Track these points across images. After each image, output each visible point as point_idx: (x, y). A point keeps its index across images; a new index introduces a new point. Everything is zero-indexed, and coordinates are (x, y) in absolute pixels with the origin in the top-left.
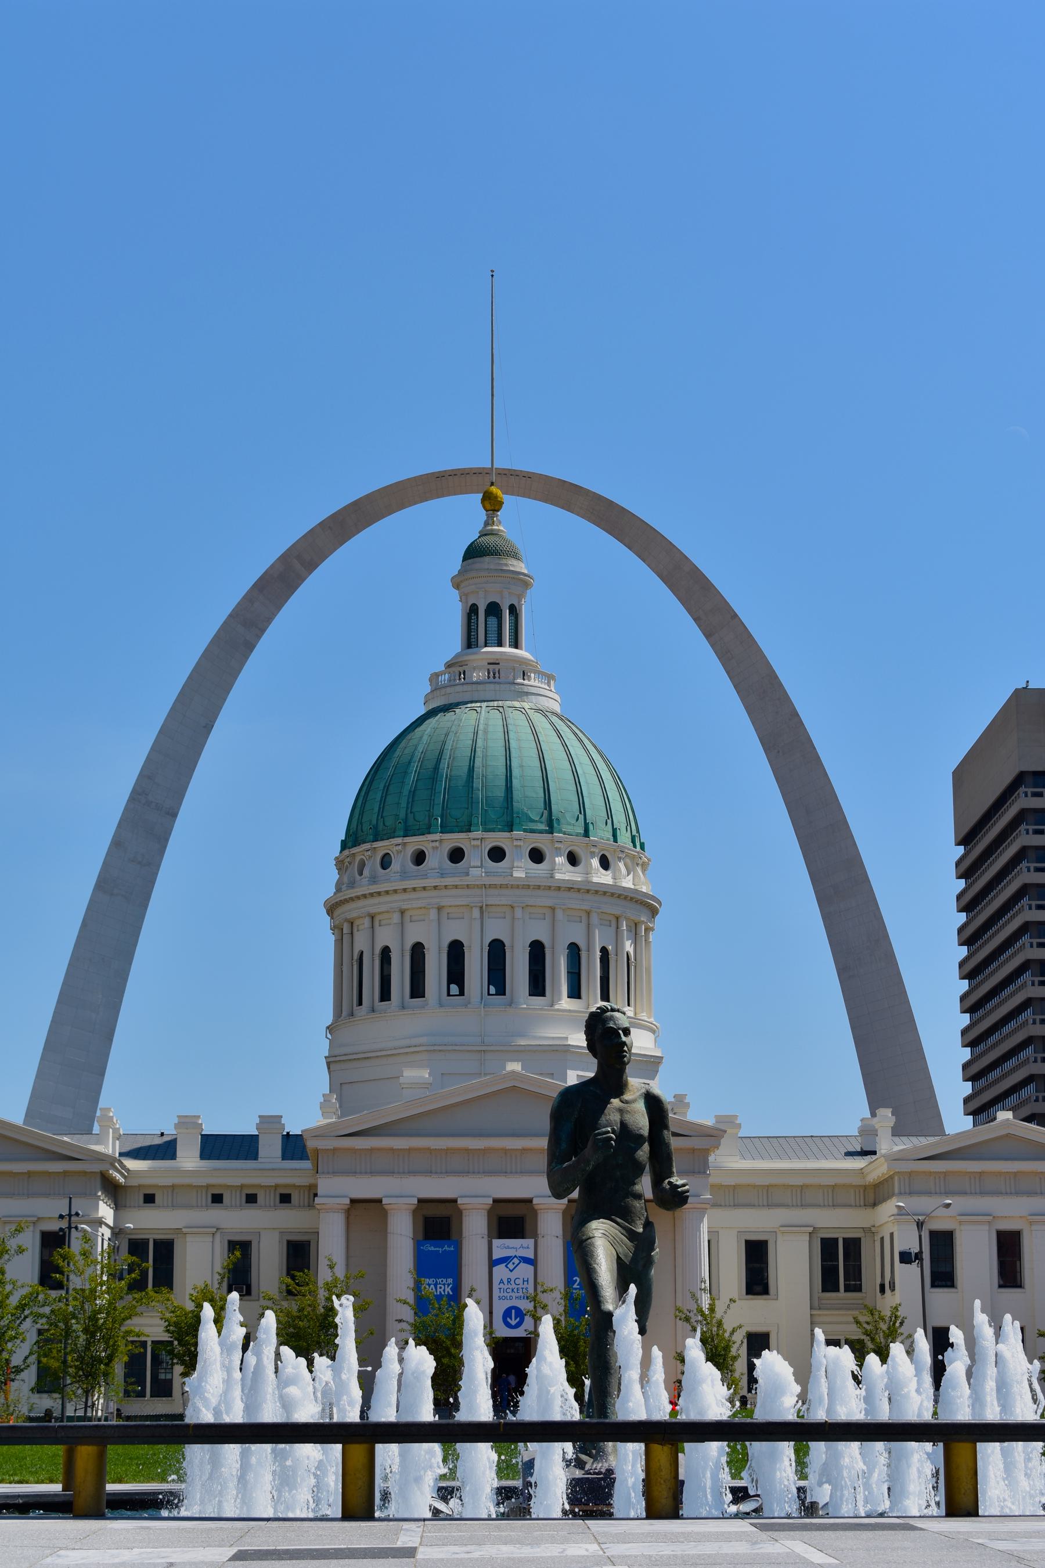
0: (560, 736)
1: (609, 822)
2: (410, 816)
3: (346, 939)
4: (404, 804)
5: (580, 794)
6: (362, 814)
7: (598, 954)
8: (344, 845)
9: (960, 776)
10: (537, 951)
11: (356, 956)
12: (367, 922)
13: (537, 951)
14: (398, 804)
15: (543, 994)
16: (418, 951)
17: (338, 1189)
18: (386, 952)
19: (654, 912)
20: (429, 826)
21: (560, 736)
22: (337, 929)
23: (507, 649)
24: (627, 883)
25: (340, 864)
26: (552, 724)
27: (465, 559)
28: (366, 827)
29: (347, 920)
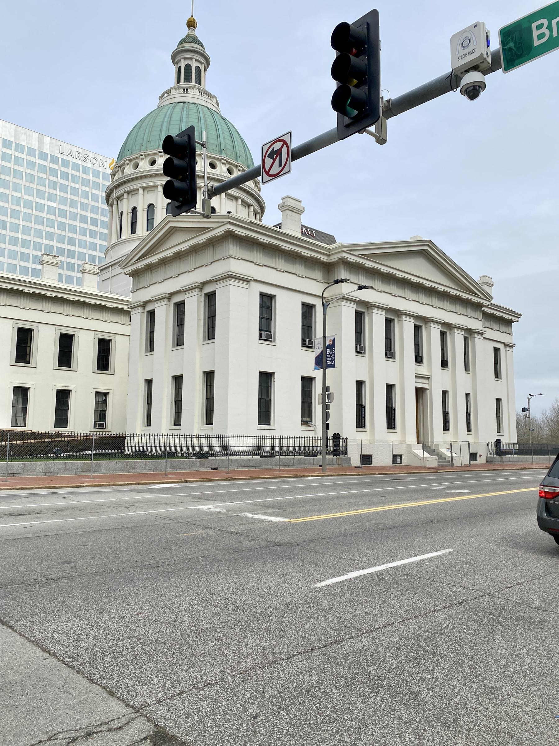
12: (115, 203)
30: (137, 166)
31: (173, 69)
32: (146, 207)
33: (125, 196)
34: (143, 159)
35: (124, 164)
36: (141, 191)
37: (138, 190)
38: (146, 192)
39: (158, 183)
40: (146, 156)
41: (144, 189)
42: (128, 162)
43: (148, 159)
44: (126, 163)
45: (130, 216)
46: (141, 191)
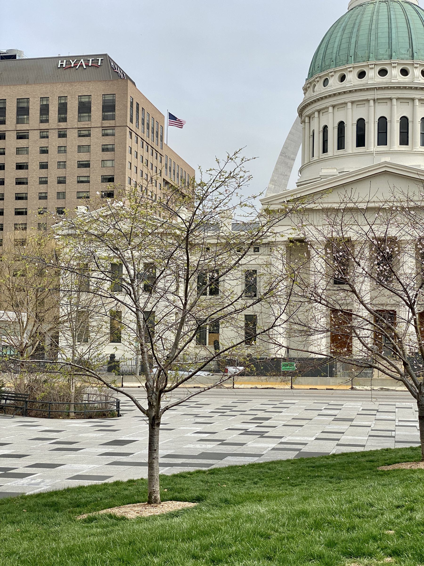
2: (338, 57)
4: (335, 51)
8: (307, 79)
10: (404, 122)
11: (311, 134)
12: (316, 114)
13: (404, 122)
15: (407, 144)
16: (341, 126)
18: (325, 127)
20: (348, 60)
22: (303, 122)
25: (305, 89)
26: (414, 8)
28: (316, 67)
29: (307, 116)
30: (343, 78)
32: (356, 122)
37: (347, 103)
39: (369, 97)
40: (354, 68)
41: (353, 102)
42: (333, 73)
44: (330, 74)
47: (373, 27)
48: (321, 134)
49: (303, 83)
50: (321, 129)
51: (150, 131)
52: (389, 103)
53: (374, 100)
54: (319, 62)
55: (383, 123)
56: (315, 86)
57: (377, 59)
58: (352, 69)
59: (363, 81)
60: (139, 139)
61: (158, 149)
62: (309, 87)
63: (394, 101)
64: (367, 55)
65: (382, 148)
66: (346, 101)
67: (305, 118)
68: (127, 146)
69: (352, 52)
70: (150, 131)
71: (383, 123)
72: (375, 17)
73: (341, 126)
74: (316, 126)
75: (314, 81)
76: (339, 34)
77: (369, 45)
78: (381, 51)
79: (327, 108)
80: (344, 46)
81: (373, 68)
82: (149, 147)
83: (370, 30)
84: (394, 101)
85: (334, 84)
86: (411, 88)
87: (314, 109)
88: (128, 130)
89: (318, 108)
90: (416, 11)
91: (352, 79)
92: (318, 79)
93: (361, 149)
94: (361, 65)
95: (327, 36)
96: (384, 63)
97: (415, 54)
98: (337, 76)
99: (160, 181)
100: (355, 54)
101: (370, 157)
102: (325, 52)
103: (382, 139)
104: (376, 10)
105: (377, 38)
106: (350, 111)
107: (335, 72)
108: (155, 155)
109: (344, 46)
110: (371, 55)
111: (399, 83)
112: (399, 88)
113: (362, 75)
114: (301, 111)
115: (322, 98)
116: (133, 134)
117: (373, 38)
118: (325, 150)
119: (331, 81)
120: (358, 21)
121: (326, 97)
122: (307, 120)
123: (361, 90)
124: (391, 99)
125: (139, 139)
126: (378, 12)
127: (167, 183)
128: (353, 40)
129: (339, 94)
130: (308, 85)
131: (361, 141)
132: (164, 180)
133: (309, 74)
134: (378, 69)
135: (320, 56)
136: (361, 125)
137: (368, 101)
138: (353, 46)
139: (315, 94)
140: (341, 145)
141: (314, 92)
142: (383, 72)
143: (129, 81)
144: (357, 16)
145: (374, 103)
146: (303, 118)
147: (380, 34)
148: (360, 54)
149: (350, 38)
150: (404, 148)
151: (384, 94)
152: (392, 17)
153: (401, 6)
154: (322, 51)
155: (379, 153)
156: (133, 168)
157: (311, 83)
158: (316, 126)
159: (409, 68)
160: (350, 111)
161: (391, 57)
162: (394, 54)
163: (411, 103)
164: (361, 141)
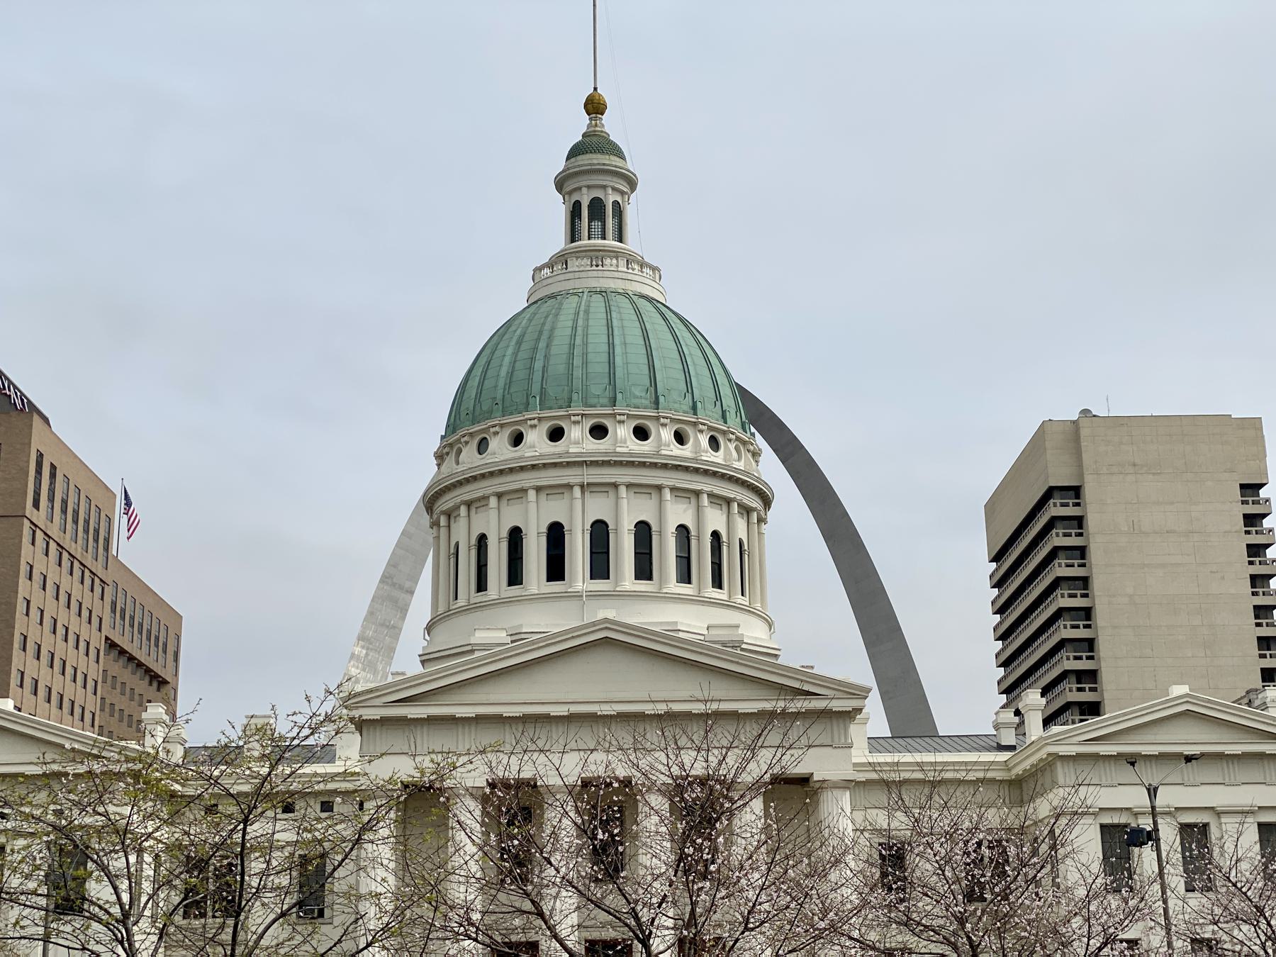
0: (665, 319)
1: (718, 403)
3: (443, 531)
4: (501, 383)
5: (686, 372)
6: (460, 405)
7: (708, 540)
8: (443, 437)
9: (992, 508)
12: (463, 510)
13: (643, 532)
14: (496, 386)
15: (650, 578)
16: (515, 537)
17: (401, 767)
18: (482, 539)
19: (767, 502)
21: (665, 319)
22: (435, 524)
23: (611, 243)
24: (740, 465)
25: (440, 457)
27: (568, 159)
29: (443, 513)
30: (517, 439)
31: (558, 210)
32: (544, 529)
33: (493, 501)
34: (534, 426)
35: (486, 430)
36: (532, 494)
38: (543, 496)
39: (572, 480)
40: (540, 419)
41: (538, 489)
42: (497, 429)
43: (545, 427)
44: (492, 430)
45: (505, 545)
46: (532, 494)
47: (578, 341)
48: (474, 553)
49: (436, 444)
50: (474, 541)
51: (81, 528)
52: (612, 494)
53: (582, 486)
54: (469, 403)
55: (600, 533)
56: (459, 451)
57: (587, 405)
58: (535, 422)
59: (560, 447)
60: (53, 546)
61: (98, 568)
62: (447, 454)
63: (623, 490)
64: (566, 395)
65: (600, 585)
66: (526, 484)
67: (438, 519)
68: (23, 562)
69: (536, 388)
70: (81, 528)
71: (600, 533)
72: (580, 322)
73: (515, 537)
74: (463, 534)
75: (458, 441)
76: (510, 351)
77: (570, 376)
78: (595, 390)
79: (485, 498)
80: (520, 374)
81: (578, 422)
82: (76, 564)
83: (572, 346)
84: (623, 490)
85: (500, 450)
86: (654, 466)
87: (458, 500)
88: (26, 522)
89: (467, 497)
90: (662, 315)
91: (536, 442)
92: (466, 438)
93: (556, 586)
94: (555, 415)
95: (487, 351)
96: (600, 412)
97: (661, 399)
98: (506, 433)
99: (97, 642)
100: (543, 392)
101: (573, 605)
102: (481, 383)
103: (600, 567)
104: (582, 308)
105: (585, 363)
106: (533, 506)
107: (502, 426)
108: (88, 581)
109: (520, 374)
110: (575, 396)
111: (630, 454)
112: (631, 464)
113: (556, 434)
114: (431, 501)
115: (475, 478)
116: (39, 534)
117: (577, 361)
118: (481, 586)
119: (494, 444)
120: (547, 327)
121: (483, 476)
122: (443, 521)
123: (555, 465)
124: (615, 486)
125: (53, 546)
126: (587, 312)
127: (112, 645)
128: (538, 365)
129: (511, 470)
130: (446, 450)
131: (556, 570)
132: (107, 638)
133: (448, 426)
134: (589, 423)
135: (472, 392)
136: (556, 535)
137: (569, 487)
138: (537, 376)
139: (460, 468)
140: (515, 577)
141: (458, 463)
142: (599, 431)
143: (36, 417)
144: (546, 317)
145: (583, 493)
146: (435, 517)
147: (590, 356)
148: (551, 392)
149: (532, 359)
150: (643, 586)
151: (602, 474)
152: (615, 323)
153: (632, 302)
154: (474, 383)
155: (594, 595)
156: (35, 614)
157: (451, 445)
158: (463, 534)
159: (651, 426)
160: (533, 506)
161: (613, 402)
162: (619, 396)
163: (655, 495)
164: (556, 570)
